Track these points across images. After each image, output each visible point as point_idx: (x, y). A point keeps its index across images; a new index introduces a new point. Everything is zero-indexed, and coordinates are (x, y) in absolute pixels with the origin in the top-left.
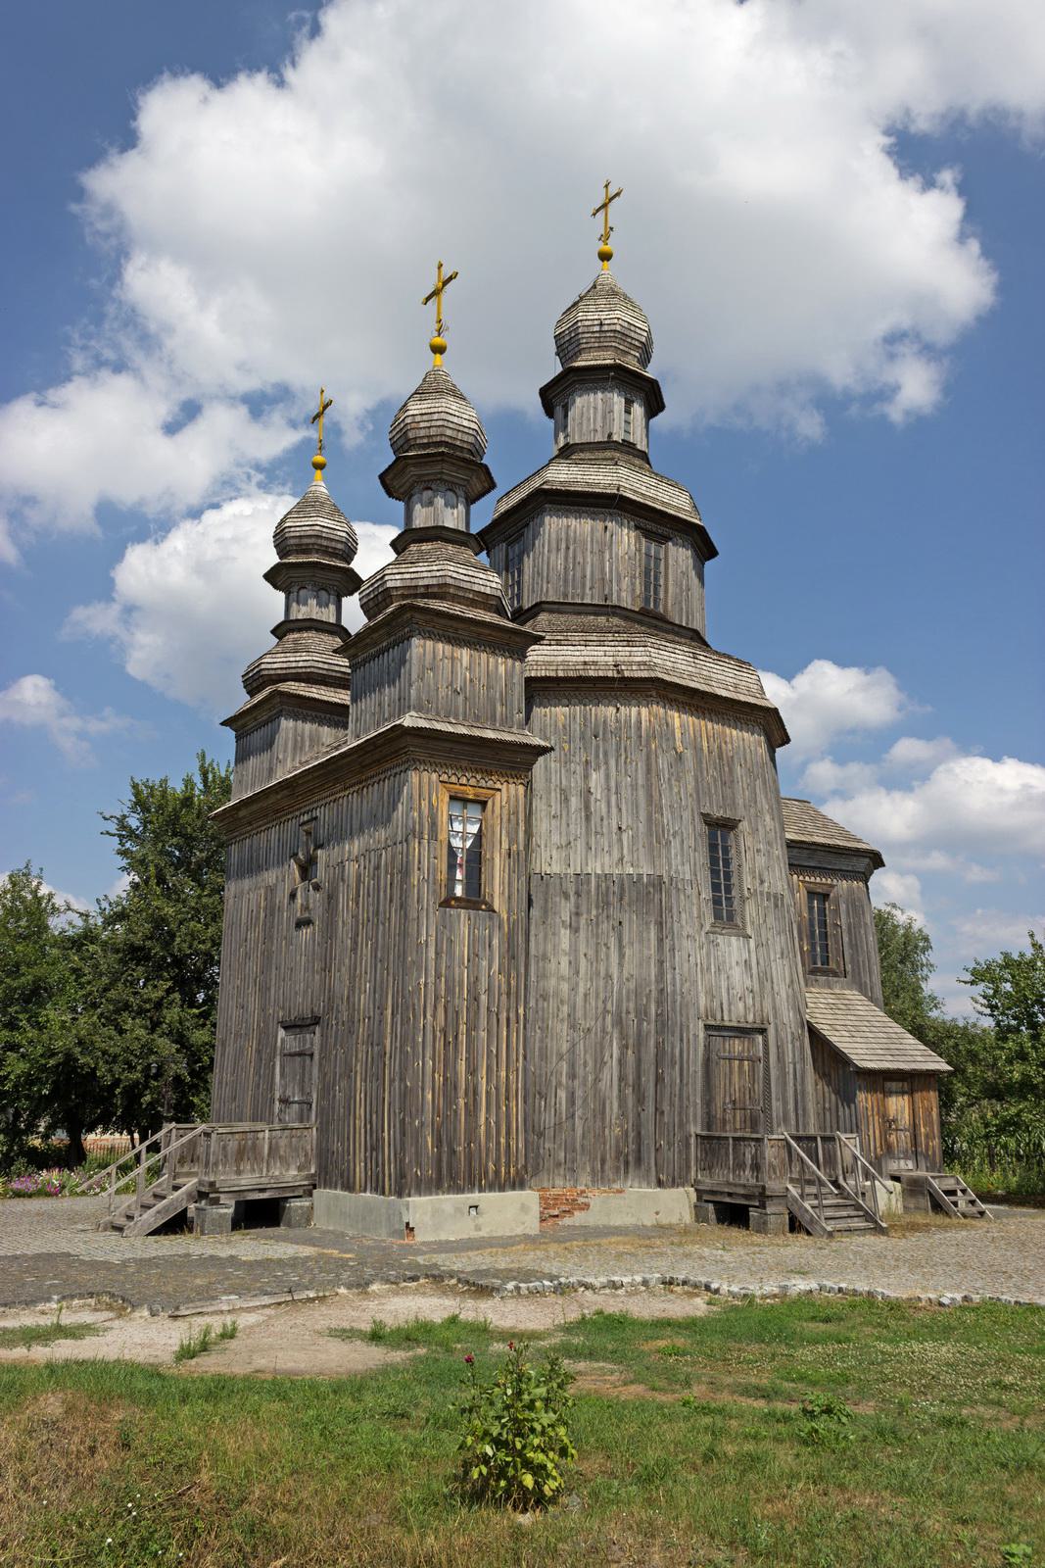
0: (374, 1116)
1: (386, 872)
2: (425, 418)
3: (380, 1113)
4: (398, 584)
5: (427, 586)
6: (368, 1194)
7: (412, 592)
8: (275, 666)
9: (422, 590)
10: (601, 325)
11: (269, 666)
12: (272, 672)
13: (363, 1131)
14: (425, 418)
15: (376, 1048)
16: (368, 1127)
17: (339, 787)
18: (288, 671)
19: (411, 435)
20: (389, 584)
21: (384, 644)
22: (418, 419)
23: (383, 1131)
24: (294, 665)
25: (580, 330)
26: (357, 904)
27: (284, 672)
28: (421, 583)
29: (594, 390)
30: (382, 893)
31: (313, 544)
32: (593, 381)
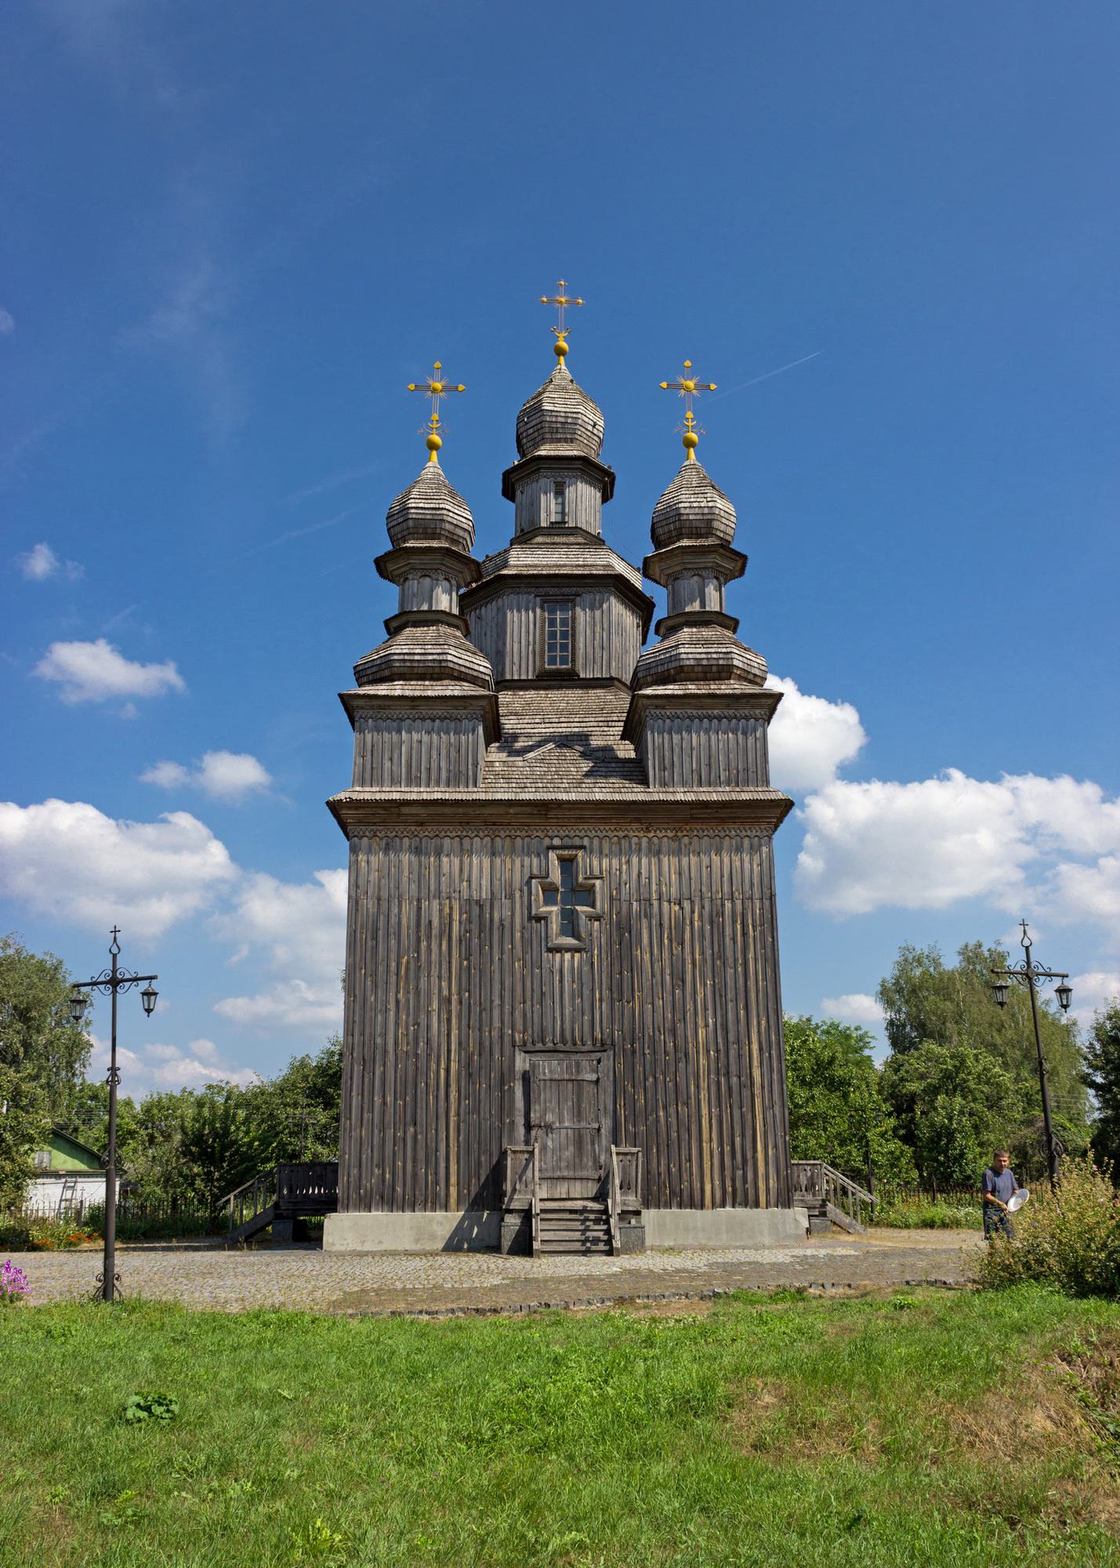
0: (738, 1140)
1: (734, 922)
2: (726, 515)
3: (749, 1133)
4: (740, 665)
5: (755, 675)
6: (728, 1209)
7: (745, 675)
8: (460, 662)
9: (751, 677)
10: (594, 427)
11: (455, 660)
12: (457, 667)
13: (716, 1153)
14: (726, 515)
15: (734, 1080)
16: (727, 1149)
17: (635, 826)
18: (471, 672)
19: (716, 524)
20: (736, 662)
21: (715, 712)
22: (722, 513)
23: (755, 1150)
24: (476, 667)
25: (580, 422)
26: (682, 944)
27: (467, 671)
28: (754, 671)
29: (591, 484)
30: (727, 939)
31: (464, 538)
32: (590, 476)
